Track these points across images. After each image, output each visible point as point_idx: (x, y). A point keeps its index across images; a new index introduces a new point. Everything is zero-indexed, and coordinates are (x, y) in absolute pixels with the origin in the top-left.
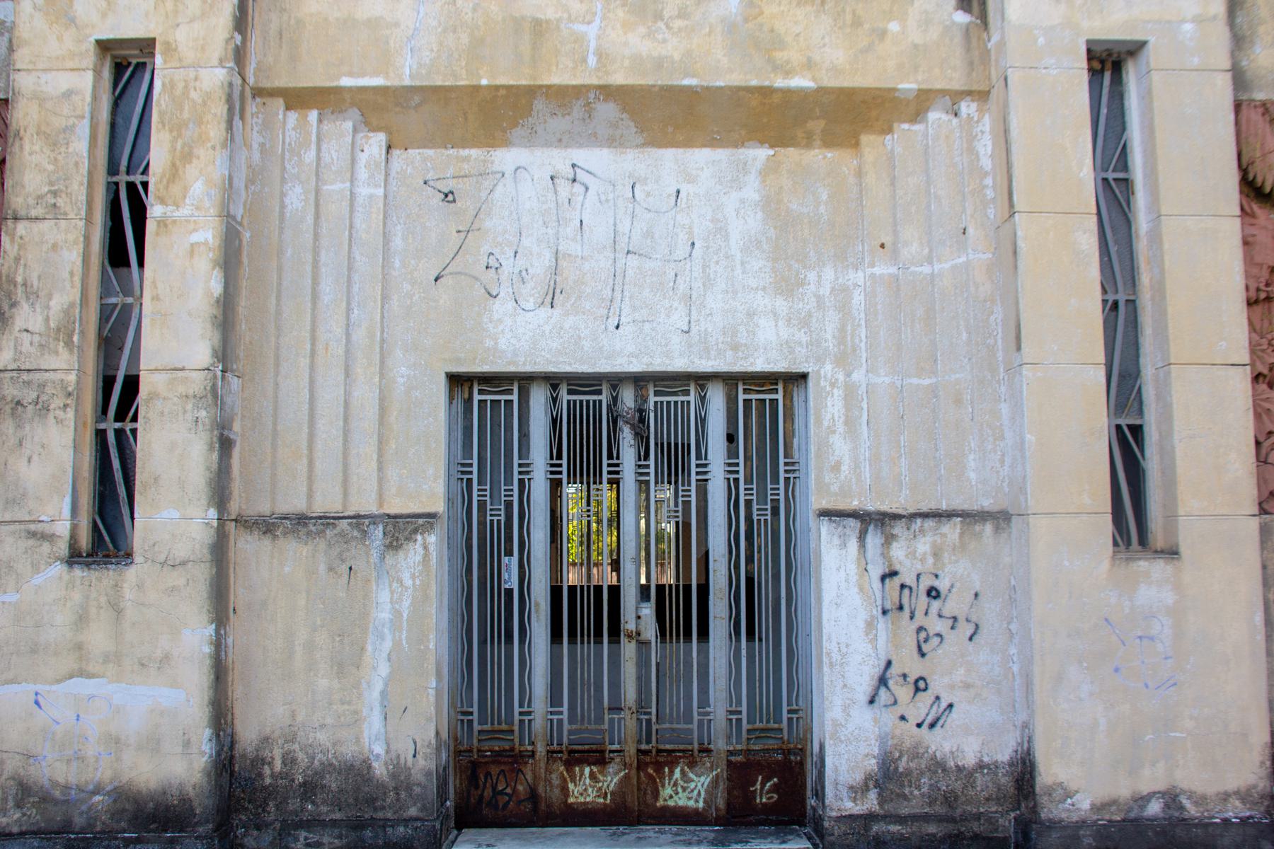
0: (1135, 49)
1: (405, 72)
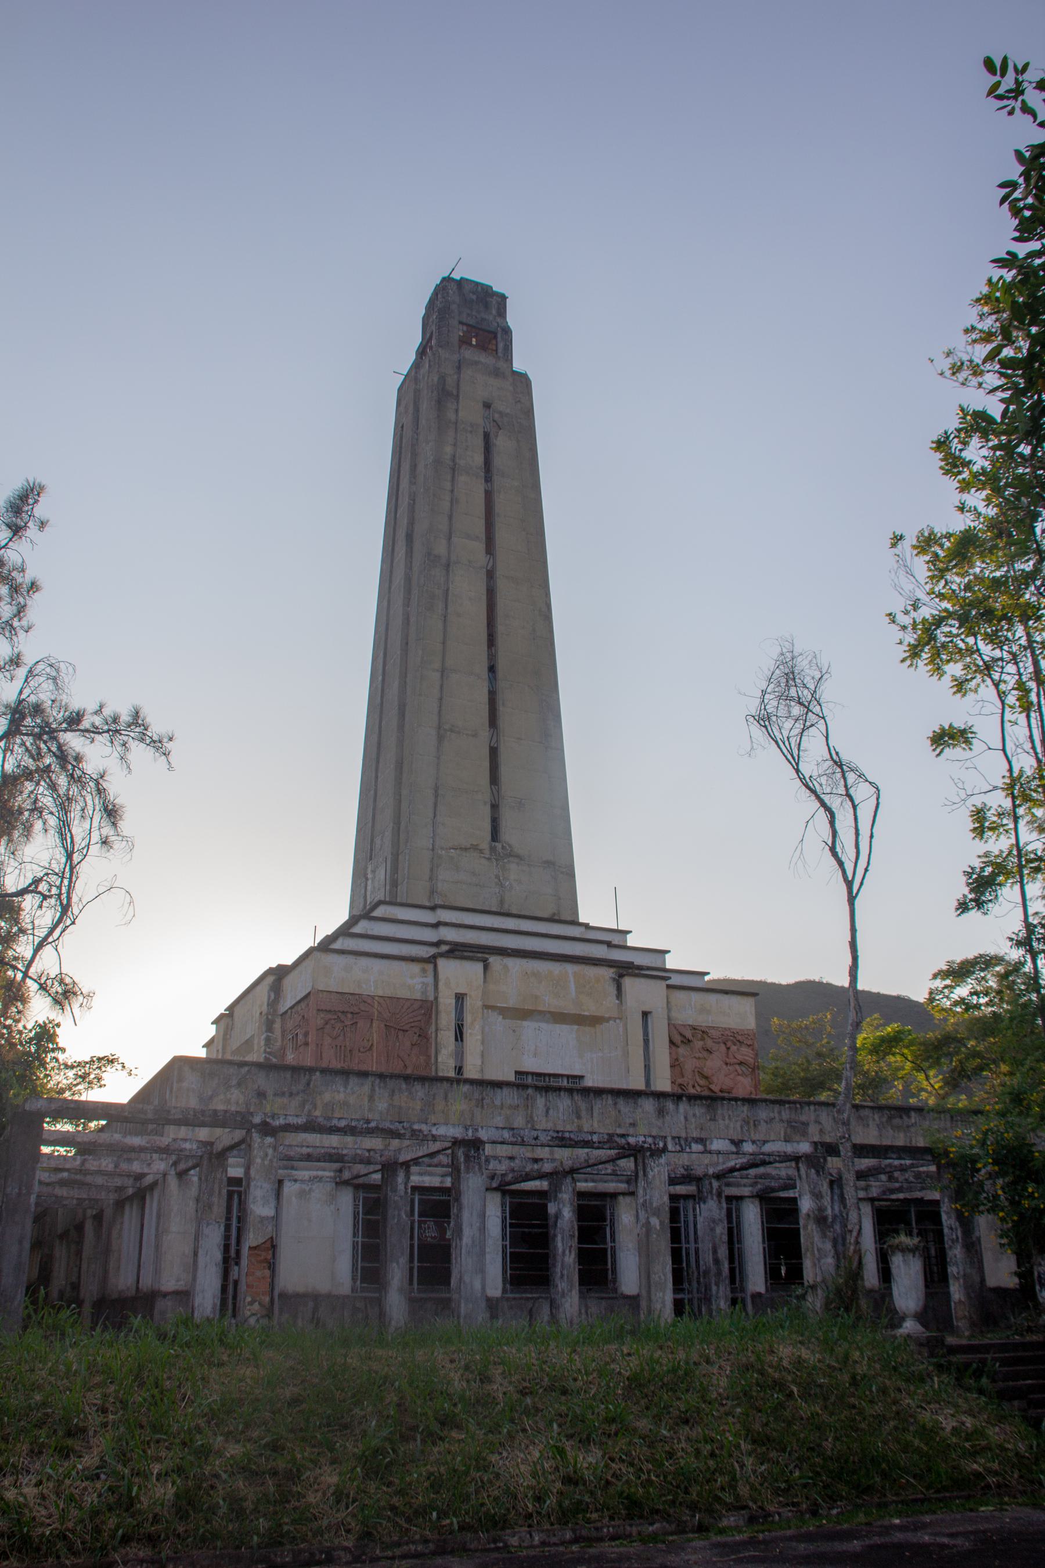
0: (650, 1012)
1: (511, 1003)
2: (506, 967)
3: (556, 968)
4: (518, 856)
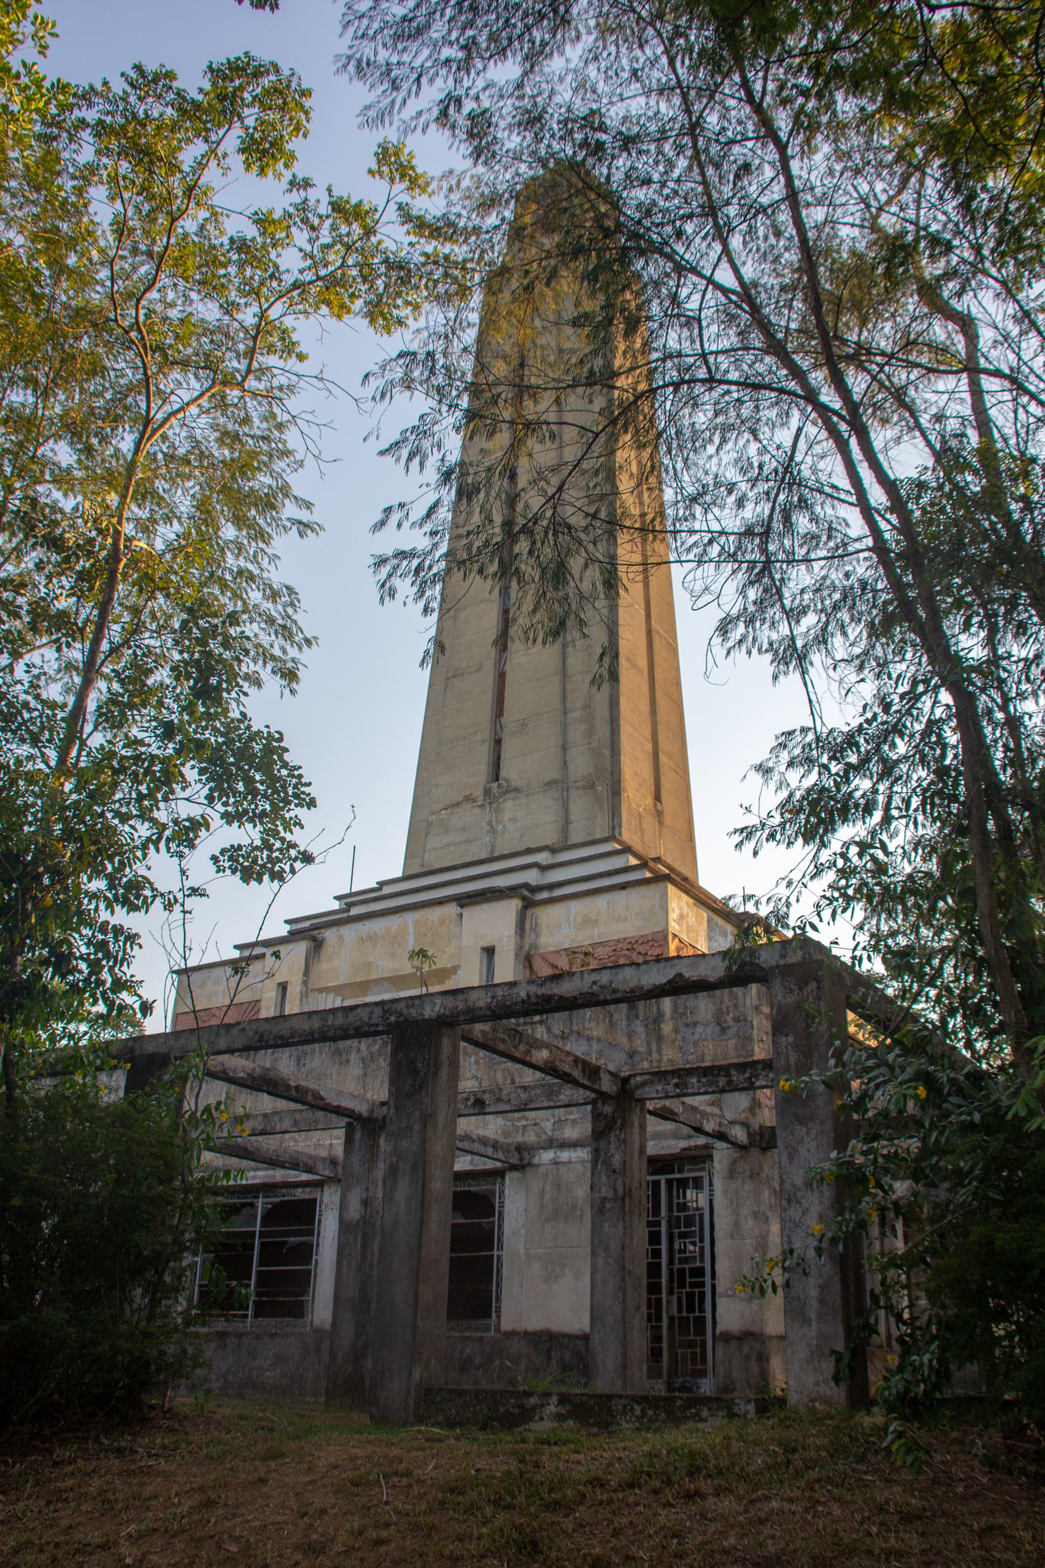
1: (342, 981)
2: (341, 939)
3: (393, 923)
4: (516, 790)
